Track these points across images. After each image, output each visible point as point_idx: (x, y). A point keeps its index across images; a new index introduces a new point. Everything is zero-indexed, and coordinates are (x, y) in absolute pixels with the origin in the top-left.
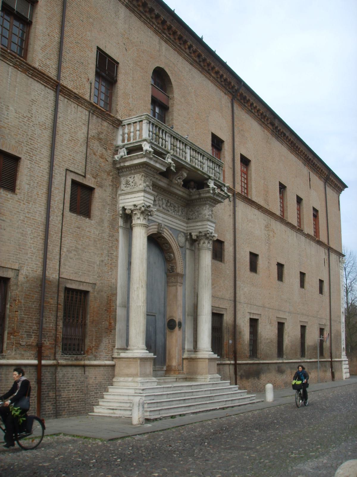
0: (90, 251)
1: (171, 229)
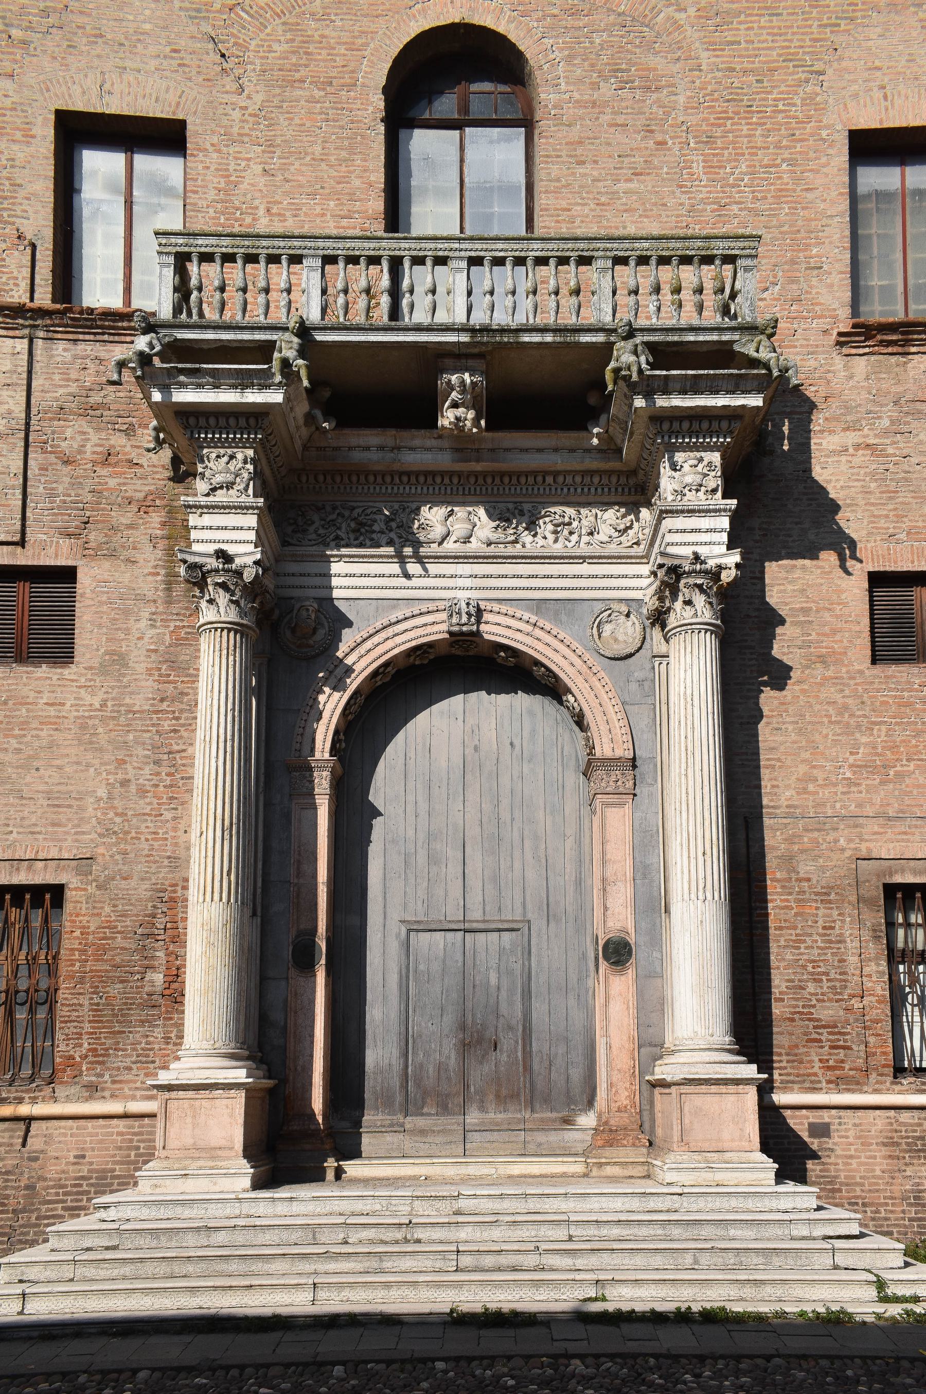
0: (58, 762)
1: (539, 606)
